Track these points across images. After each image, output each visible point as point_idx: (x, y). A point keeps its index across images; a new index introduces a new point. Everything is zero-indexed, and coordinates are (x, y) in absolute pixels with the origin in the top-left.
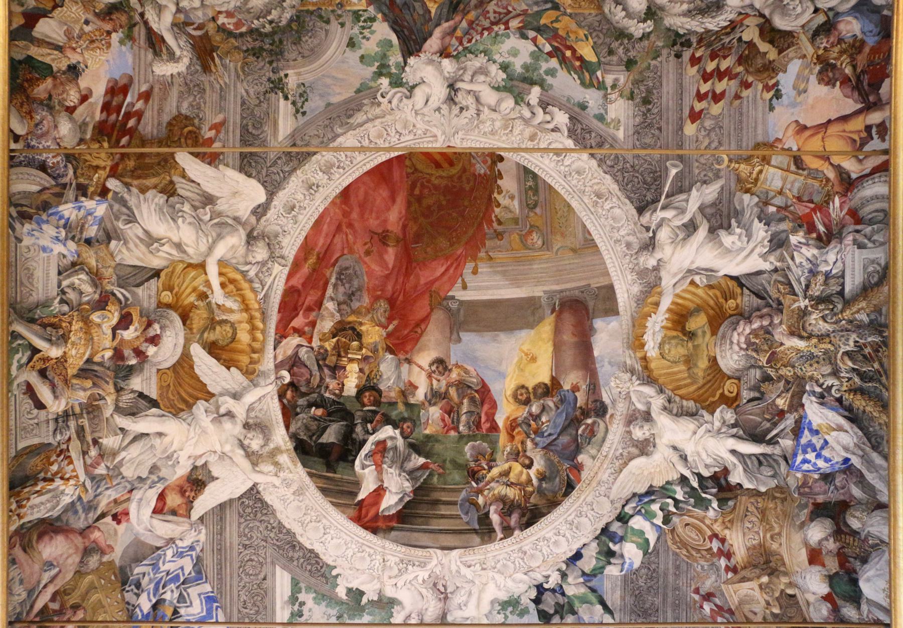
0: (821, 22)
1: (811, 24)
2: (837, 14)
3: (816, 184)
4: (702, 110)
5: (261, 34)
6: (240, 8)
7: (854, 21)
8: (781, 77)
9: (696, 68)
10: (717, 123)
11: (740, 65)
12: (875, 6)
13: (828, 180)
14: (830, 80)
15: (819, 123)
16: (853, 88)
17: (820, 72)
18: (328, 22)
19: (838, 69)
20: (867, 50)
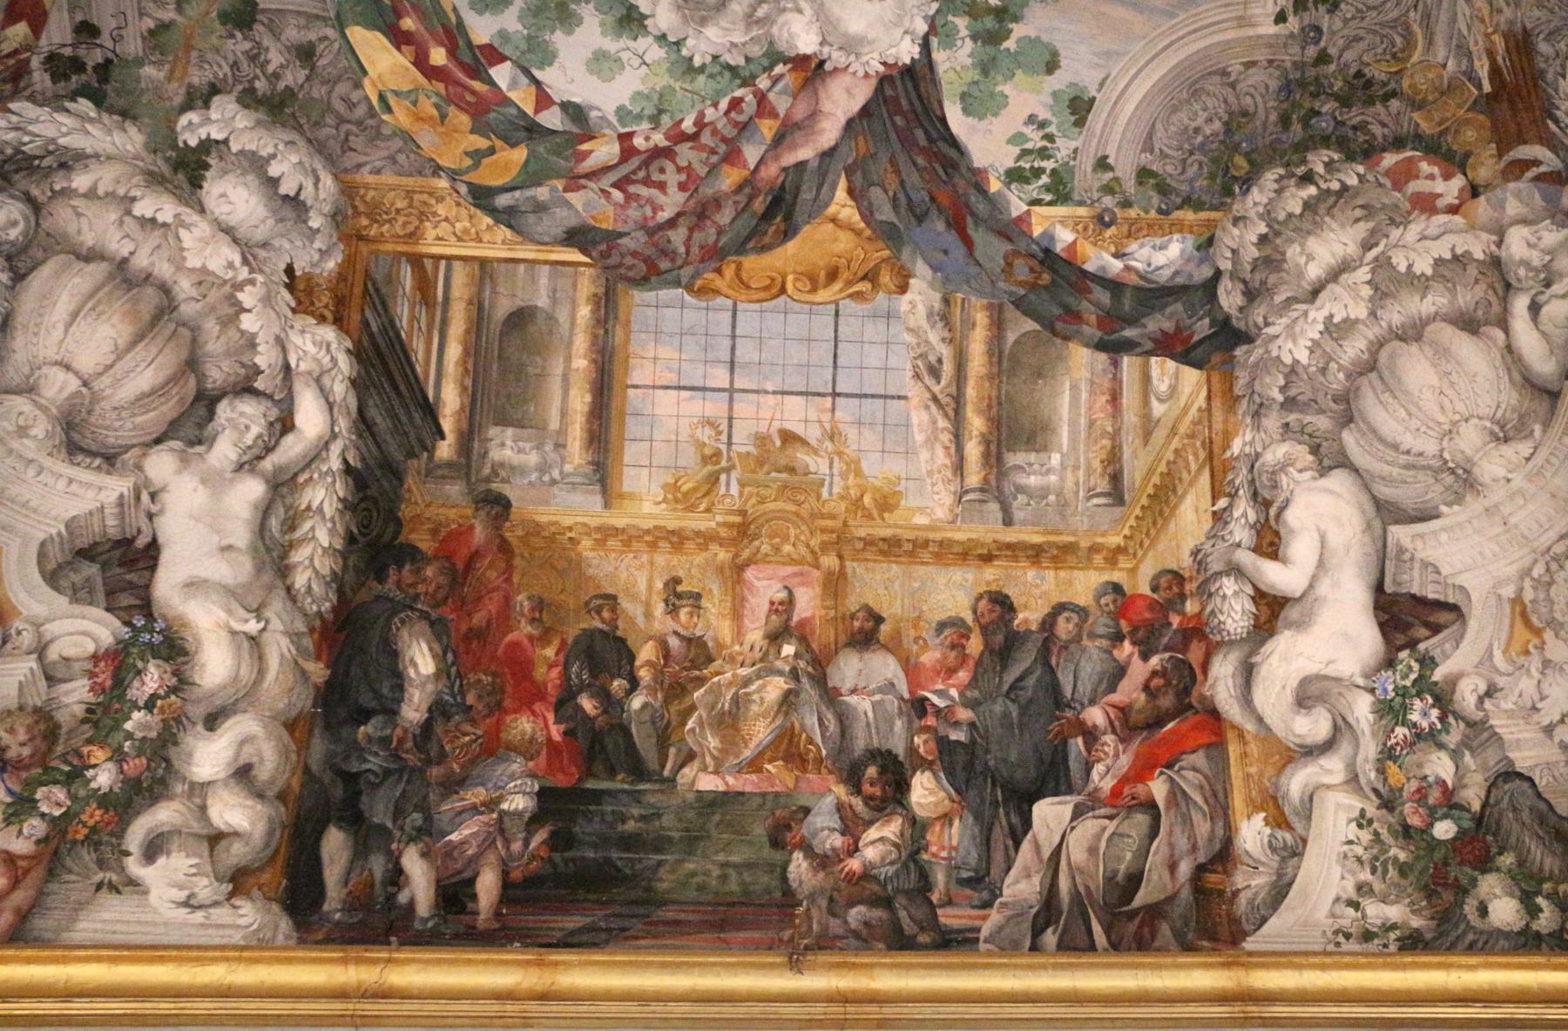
5: (1342, 144)
6: (1392, 222)
18: (1144, 174)
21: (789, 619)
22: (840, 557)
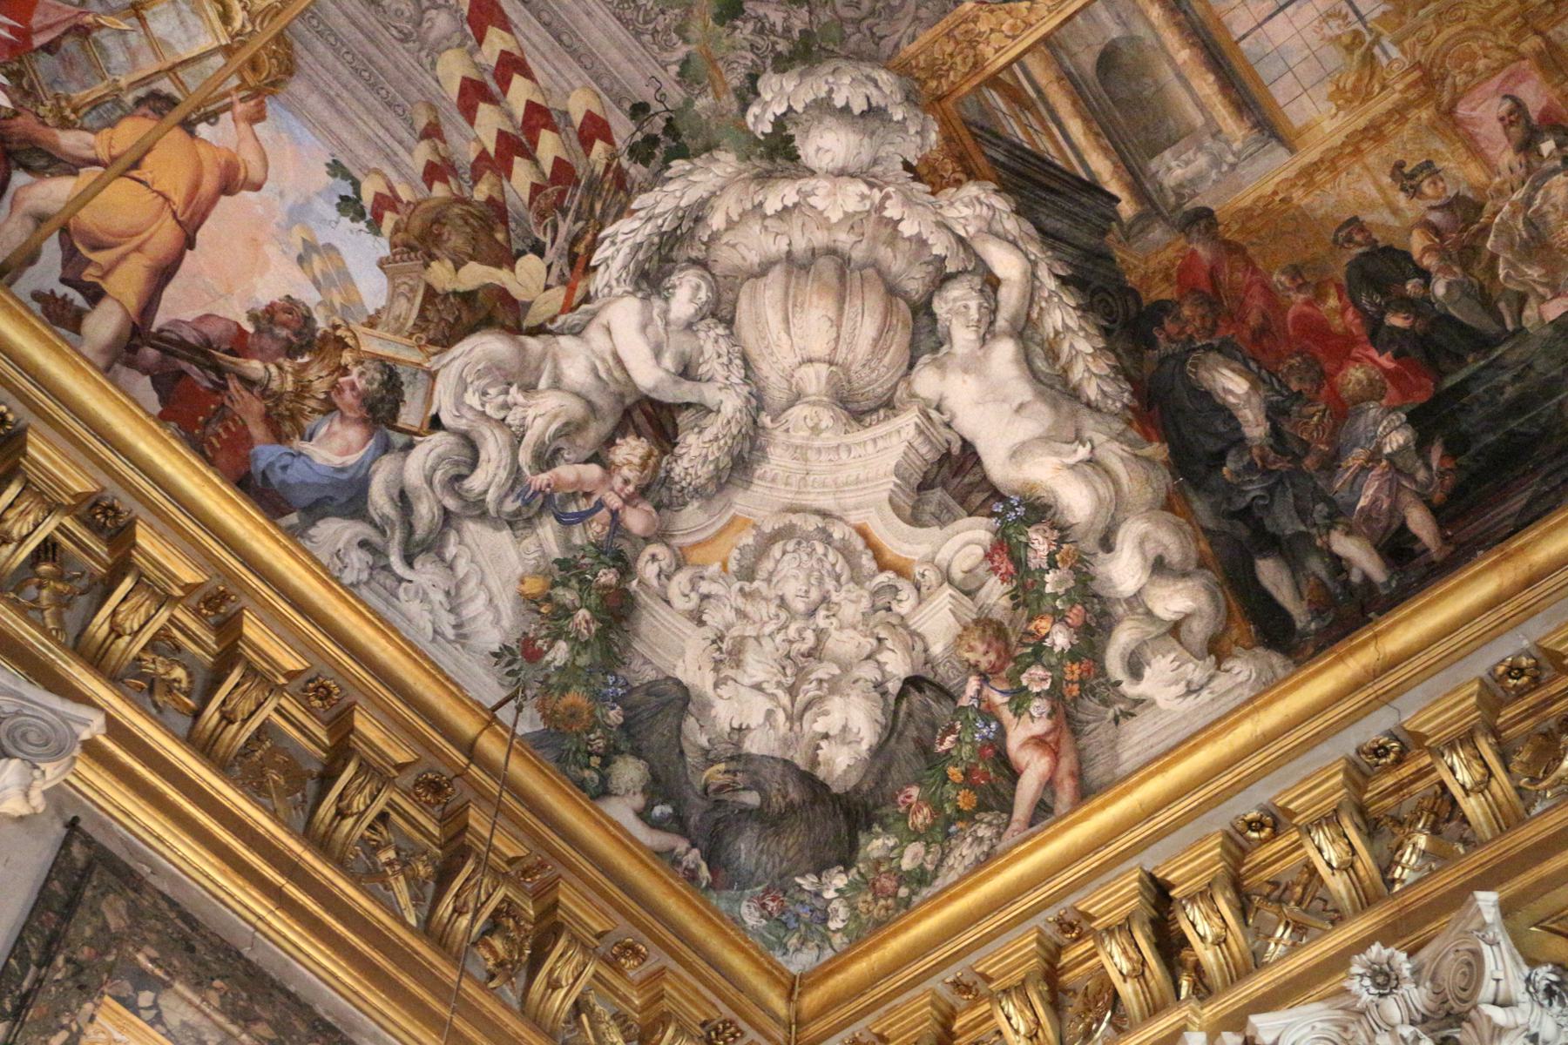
0: (403, 410)
1: (421, 393)
2: (387, 448)
3: (79, 95)
4: (480, 41)
7: (337, 461)
8: (382, 247)
9: (578, 118)
10: (422, 40)
11: (490, 201)
12: (324, 516)
13: (65, 124)
14: (271, 320)
15: (208, 223)
16: (209, 344)
17: (308, 319)
19: (279, 355)
20: (258, 431)
21: (1528, 120)
22: (1537, 32)
